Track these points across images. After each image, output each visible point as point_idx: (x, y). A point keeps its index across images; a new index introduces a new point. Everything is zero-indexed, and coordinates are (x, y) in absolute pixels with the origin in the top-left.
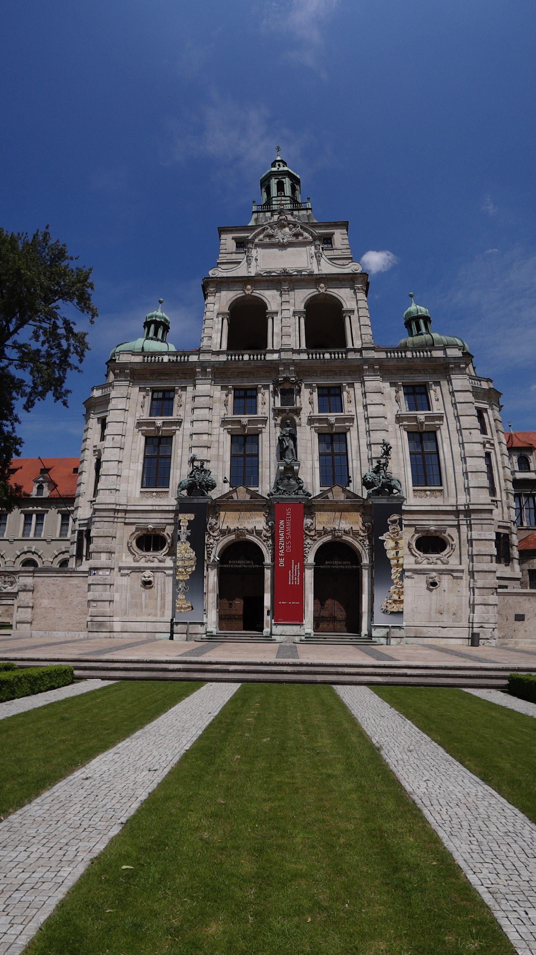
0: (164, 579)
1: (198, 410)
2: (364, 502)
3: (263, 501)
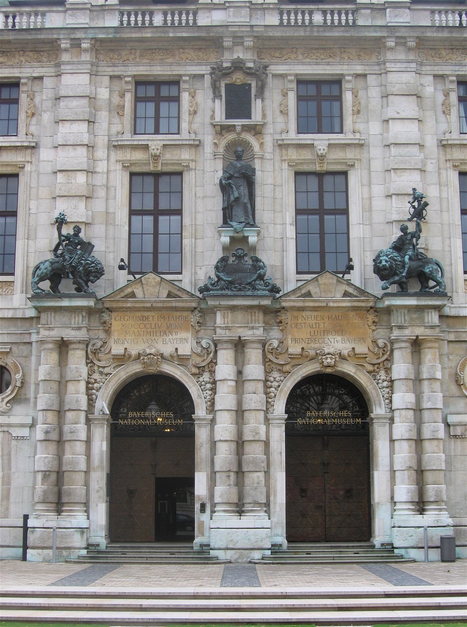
0: (9, 445)
1: (67, 125)
2: (375, 302)
3: (192, 301)
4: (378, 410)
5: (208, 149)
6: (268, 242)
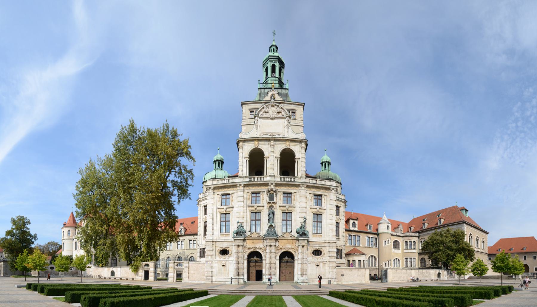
4: (296, 258)
5: (266, 207)
6: (276, 226)
